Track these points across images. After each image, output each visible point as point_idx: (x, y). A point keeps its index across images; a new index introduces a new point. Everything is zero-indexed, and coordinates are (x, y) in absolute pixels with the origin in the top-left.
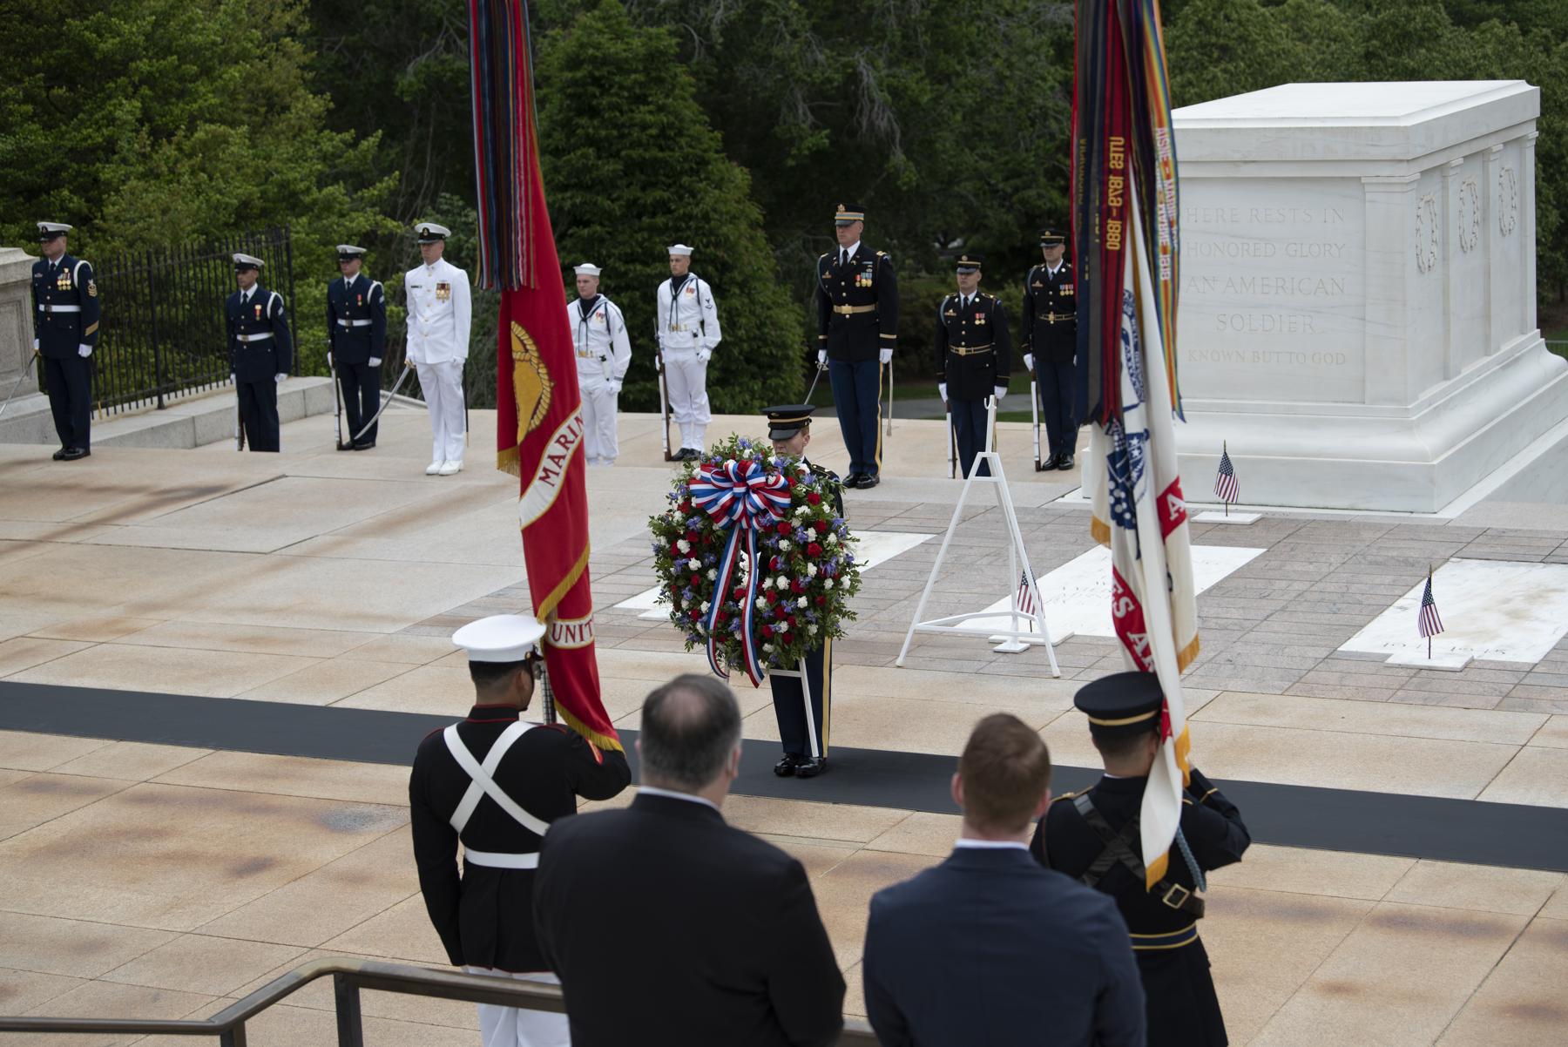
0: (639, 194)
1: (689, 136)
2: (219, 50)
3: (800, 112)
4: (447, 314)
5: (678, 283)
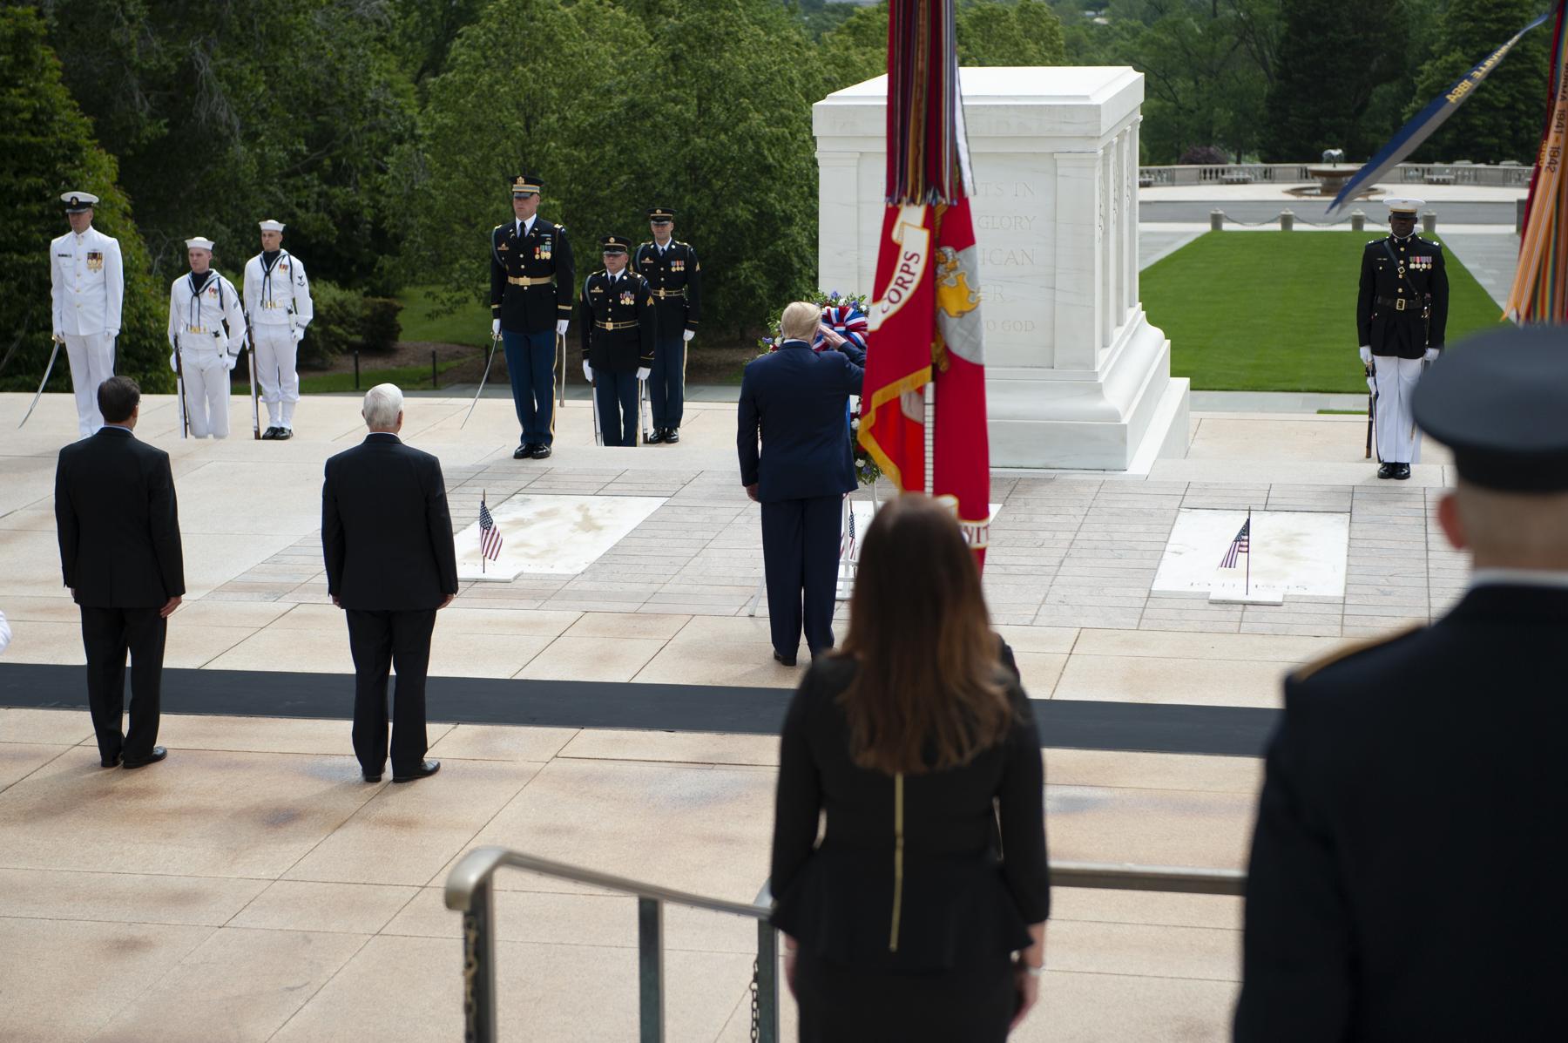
0: (13, 180)
1: (60, 121)
3: (137, 100)
4: (100, 284)
5: (270, 259)
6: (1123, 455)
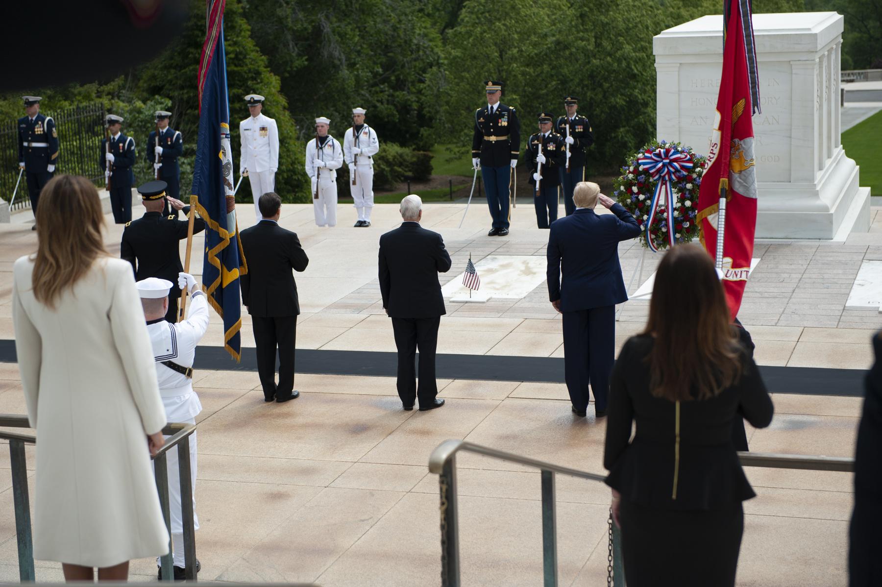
1: (250, 58)
3: (291, 46)
5: (358, 128)
6: (830, 230)
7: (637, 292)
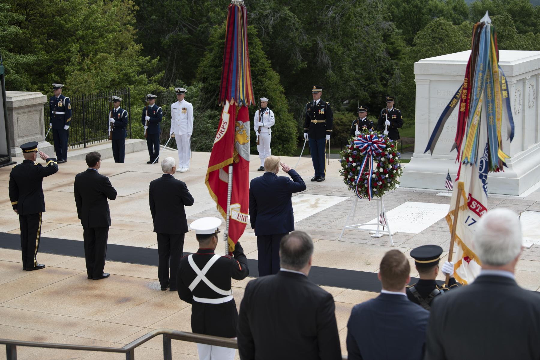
1: (261, 62)
2: (106, 28)
3: (298, 55)
7: (371, 221)
